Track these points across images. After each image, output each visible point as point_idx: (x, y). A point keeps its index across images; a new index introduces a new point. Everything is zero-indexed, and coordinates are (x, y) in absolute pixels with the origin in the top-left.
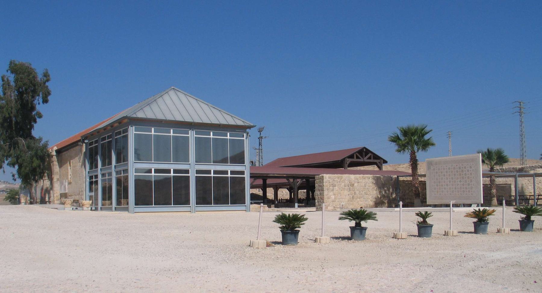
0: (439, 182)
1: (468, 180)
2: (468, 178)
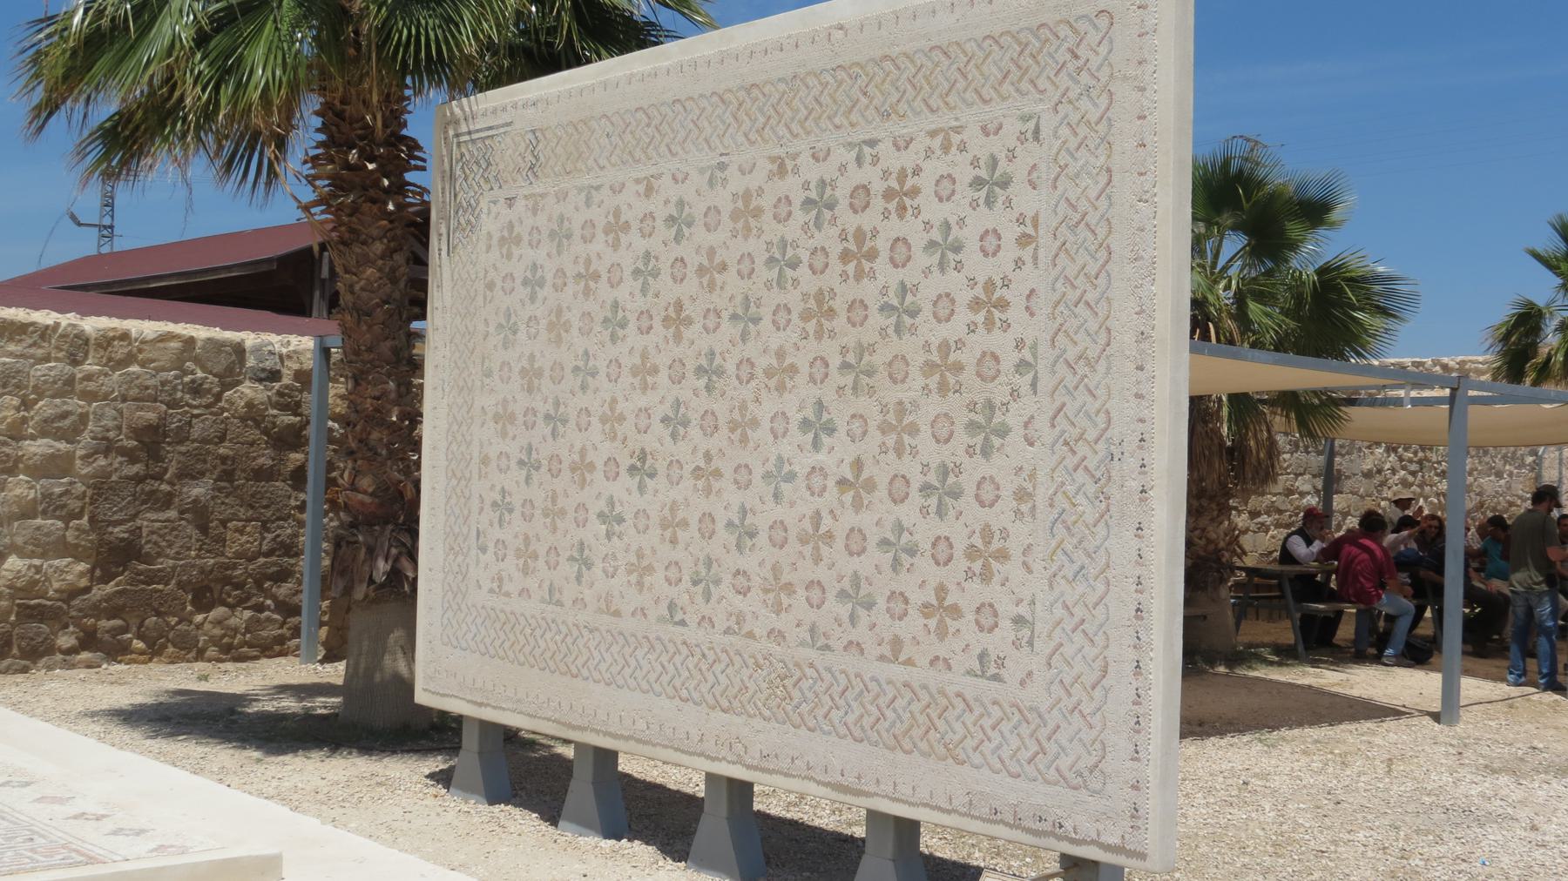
1: (932, 406)
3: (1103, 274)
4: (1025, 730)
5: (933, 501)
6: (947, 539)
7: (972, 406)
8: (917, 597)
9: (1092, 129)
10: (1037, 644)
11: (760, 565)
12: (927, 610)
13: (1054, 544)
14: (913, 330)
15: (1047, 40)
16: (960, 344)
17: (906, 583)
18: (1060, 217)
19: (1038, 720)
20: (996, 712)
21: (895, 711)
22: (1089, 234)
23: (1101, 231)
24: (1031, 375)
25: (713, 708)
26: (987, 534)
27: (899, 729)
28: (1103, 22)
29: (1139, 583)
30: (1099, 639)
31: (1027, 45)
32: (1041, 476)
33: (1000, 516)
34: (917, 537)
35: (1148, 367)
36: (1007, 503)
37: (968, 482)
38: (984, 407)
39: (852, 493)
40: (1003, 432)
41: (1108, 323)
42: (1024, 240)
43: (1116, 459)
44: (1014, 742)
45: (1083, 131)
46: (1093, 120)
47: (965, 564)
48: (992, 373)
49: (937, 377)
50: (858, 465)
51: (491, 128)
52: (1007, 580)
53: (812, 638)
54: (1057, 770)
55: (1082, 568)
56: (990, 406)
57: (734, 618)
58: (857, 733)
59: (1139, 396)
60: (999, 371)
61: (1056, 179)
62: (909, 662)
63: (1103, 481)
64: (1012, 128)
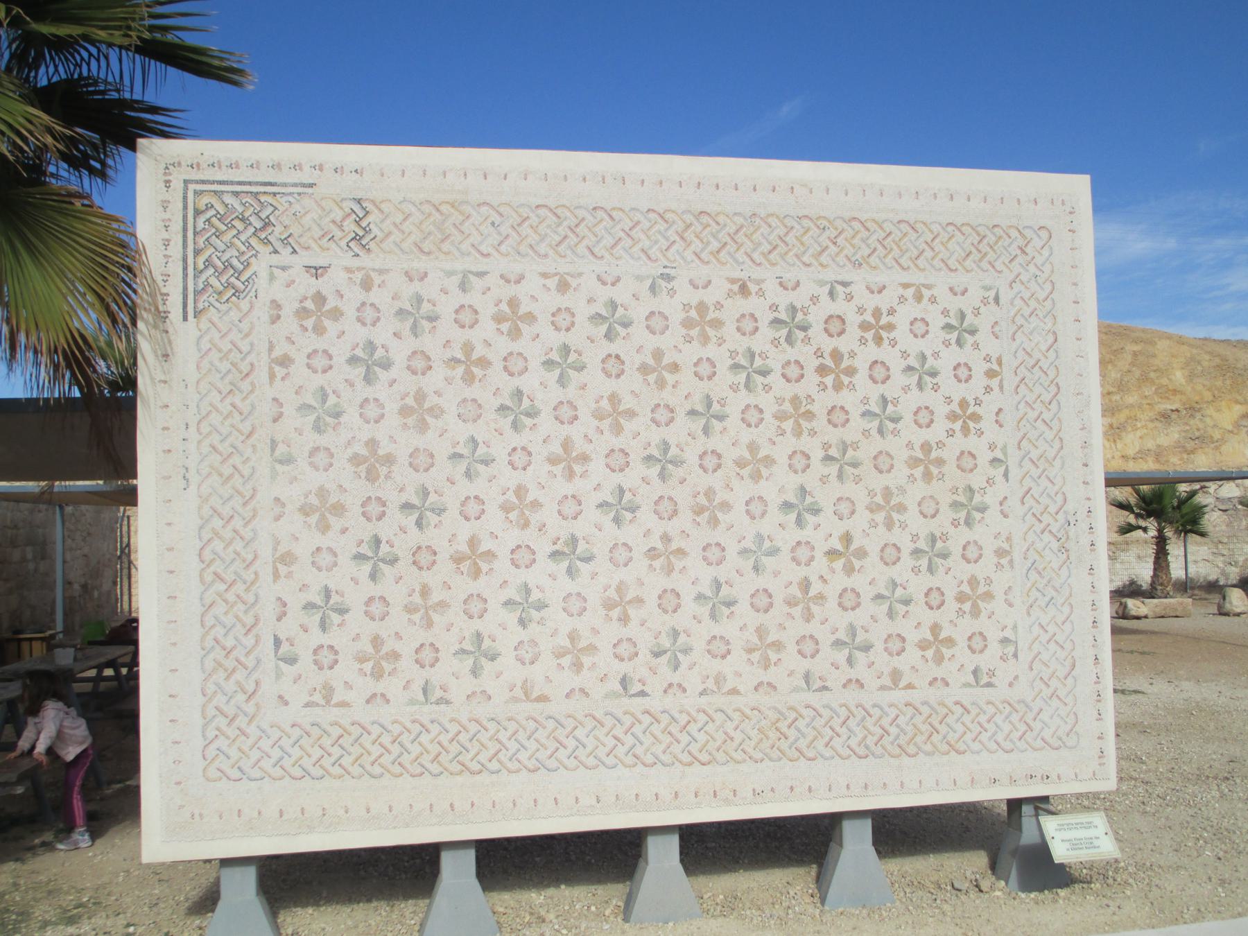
1: (918, 491)
3: (1054, 402)
4: (1015, 718)
5: (924, 562)
6: (938, 589)
7: (955, 490)
8: (913, 637)
9: (1039, 303)
12: (923, 646)
13: (1029, 585)
15: (1000, 237)
16: (940, 445)
17: (904, 627)
20: (991, 710)
21: (898, 726)
22: (1043, 375)
23: (1052, 374)
24: (1004, 468)
25: (690, 764)
26: (973, 582)
28: (1044, 234)
29: (1094, 605)
30: (1068, 645)
31: (984, 237)
33: (984, 569)
35: (1090, 464)
36: (989, 559)
38: (965, 490)
39: (843, 560)
40: (982, 509)
41: (1061, 434)
42: (991, 374)
43: (1072, 525)
44: (1007, 727)
45: (1033, 304)
46: (1041, 299)
47: (956, 606)
48: (970, 466)
49: (921, 469)
50: (847, 538)
52: (993, 613)
53: (808, 685)
54: (1043, 739)
56: (970, 490)
57: (711, 680)
58: (862, 751)
59: (1085, 483)
60: (976, 464)
61: (1014, 334)
62: (910, 686)
63: (1063, 540)
64: (975, 295)
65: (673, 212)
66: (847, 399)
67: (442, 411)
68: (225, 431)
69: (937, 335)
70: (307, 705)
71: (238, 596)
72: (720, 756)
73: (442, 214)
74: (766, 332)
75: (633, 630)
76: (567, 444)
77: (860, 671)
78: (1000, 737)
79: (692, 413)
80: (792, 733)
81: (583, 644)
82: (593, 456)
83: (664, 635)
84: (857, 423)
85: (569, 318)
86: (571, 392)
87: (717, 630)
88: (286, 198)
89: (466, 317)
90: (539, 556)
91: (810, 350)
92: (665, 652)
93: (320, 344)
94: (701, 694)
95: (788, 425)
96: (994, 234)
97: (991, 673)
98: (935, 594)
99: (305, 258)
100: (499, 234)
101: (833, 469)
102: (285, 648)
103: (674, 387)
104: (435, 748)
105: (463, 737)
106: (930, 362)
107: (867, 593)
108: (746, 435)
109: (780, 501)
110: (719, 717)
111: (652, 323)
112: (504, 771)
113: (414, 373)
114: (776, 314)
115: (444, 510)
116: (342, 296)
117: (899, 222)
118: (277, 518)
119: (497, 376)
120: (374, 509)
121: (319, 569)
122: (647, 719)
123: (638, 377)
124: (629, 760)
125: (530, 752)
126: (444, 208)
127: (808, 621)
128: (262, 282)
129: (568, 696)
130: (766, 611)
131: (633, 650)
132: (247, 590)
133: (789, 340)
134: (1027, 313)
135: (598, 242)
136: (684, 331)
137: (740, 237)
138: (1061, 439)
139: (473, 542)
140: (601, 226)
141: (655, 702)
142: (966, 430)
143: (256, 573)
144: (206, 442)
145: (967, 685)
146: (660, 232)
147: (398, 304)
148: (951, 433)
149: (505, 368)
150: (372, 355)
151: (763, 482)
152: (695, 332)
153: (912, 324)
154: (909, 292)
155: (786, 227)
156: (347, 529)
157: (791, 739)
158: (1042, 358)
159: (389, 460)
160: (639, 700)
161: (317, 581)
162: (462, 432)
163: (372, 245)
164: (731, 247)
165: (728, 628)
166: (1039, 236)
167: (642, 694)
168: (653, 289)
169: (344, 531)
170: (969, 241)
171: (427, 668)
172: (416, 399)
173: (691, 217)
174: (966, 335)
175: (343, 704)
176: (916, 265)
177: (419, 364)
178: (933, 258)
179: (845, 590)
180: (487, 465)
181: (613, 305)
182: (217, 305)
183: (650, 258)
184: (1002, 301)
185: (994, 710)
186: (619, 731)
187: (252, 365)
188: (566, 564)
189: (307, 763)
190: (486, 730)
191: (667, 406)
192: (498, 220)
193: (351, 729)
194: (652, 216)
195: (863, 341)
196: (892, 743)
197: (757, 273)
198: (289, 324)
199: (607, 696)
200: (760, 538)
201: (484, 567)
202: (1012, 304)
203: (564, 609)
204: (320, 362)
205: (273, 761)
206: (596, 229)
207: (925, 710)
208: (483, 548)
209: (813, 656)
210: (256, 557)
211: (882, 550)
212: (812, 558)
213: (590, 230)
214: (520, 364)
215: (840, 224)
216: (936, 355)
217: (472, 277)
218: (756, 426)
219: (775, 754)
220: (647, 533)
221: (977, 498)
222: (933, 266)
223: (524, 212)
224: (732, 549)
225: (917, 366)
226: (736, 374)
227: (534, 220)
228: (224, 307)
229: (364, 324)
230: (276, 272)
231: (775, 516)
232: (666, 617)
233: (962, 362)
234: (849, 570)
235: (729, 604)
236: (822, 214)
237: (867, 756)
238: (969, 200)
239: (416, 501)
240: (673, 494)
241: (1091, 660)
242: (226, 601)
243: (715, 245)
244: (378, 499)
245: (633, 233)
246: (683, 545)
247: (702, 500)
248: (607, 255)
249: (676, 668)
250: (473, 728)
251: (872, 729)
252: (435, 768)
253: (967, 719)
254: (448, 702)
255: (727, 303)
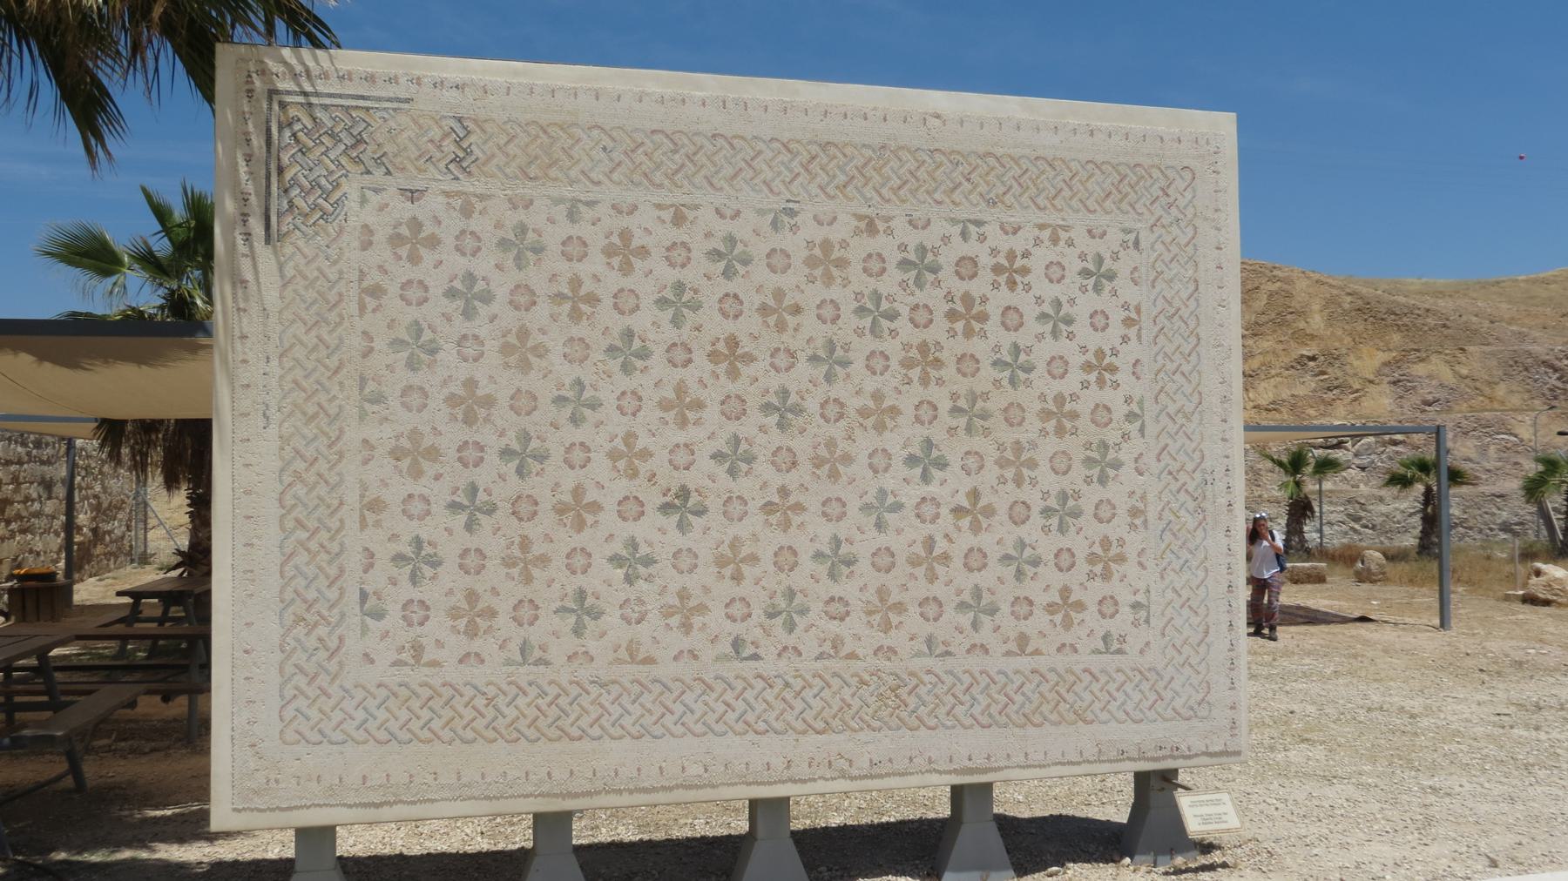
0: (523, 457)
1: (1050, 445)
2: (1059, 415)
3: (1194, 354)
4: (1145, 686)
5: (1055, 521)
7: (1088, 446)
8: (1041, 599)
9: (1181, 249)
10: (1152, 620)
11: (861, 590)
12: (1051, 608)
14: (1028, 384)
16: (1074, 397)
17: (1032, 589)
18: (1159, 308)
19: (1155, 677)
20: (1120, 678)
21: (1023, 694)
23: (1192, 324)
25: (804, 732)
27: (1028, 709)
28: (1187, 175)
30: (1202, 611)
32: (1150, 497)
34: (1039, 551)
36: (1123, 517)
37: (1087, 505)
39: (969, 518)
40: (1117, 465)
42: (1129, 322)
47: (1087, 568)
48: (1105, 420)
49: (1053, 422)
50: (975, 495)
51: (363, 98)
53: (930, 648)
55: (1187, 561)
56: (1104, 446)
57: (828, 644)
58: (985, 720)
59: (1224, 440)
61: (1154, 281)
62: (1037, 652)
64: (1114, 237)
65: (798, 142)
66: (978, 347)
67: (547, 351)
68: (310, 365)
69: (1073, 280)
70: (394, 664)
71: (322, 546)
72: (836, 723)
73: (550, 137)
74: (894, 275)
75: (746, 589)
76: (681, 389)
77: (986, 635)
78: (1129, 707)
79: (814, 359)
80: (912, 701)
81: (692, 603)
82: (708, 402)
83: (779, 594)
84: (987, 372)
85: (684, 254)
86: (686, 333)
87: (836, 590)
88: (379, 114)
89: (574, 249)
90: (648, 509)
91: (940, 293)
92: (780, 613)
93: (415, 273)
94: (817, 659)
95: (915, 373)
96: (1135, 174)
97: (1122, 639)
98: (1065, 556)
99: (401, 180)
100: (611, 160)
101: (962, 421)
102: (371, 602)
103: (796, 330)
104: (532, 712)
105: (563, 701)
106: (1066, 309)
107: (994, 553)
108: (871, 385)
109: (905, 453)
110: (835, 682)
111: (774, 261)
112: (606, 737)
113: (517, 308)
114: (905, 255)
115: (546, 458)
116: (440, 223)
117: (1037, 158)
118: (366, 462)
119: (606, 313)
120: (470, 454)
121: (411, 517)
122: (760, 684)
123: (757, 319)
124: (740, 727)
125: (634, 717)
126: (552, 130)
127: (931, 582)
128: (352, 204)
129: (676, 658)
130: (888, 571)
131: (745, 610)
132: (332, 539)
133: (919, 283)
134: (1167, 260)
135: (716, 173)
136: (807, 271)
137: (869, 171)
138: (1200, 393)
139: (578, 492)
140: (721, 154)
141: (768, 667)
142: (1101, 382)
143: (341, 521)
144: (289, 378)
145: (1097, 651)
146: (783, 163)
147: (500, 233)
148: (1085, 385)
149: (616, 306)
150: (472, 287)
151: (887, 434)
152: (818, 272)
153: (1047, 267)
154: (1046, 234)
155: (917, 161)
156: (441, 475)
157: (911, 707)
158: (1183, 307)
159: (489, 402)
160: (752, 664)
161: (408, 529)
162: (568, 373)
163: (473, 168)
164: (859, 181)
165: (847, 588)
166: (1181, 177)
167: (755, 657)
168: (775, 225)
169: (437, 477)
170: (1109, 180)
171: (526, 626)
172: (518, 338)
173: (818, 149)
174: (1104, 281)
175: (434, 664)
176: (1053, 205)
177: (523, 300)
178: (1071, 198)
179: (971, 550)
180: (594, 409)
181: (731, 240)
182: (303, 228)
183: (771, 191)
184: (1143, 244)
185: (1124, 678)
186: (729, 696)
187: (340, 295)
188: (676, 517)
189: (394, 726)
190: (588, 693)
191: (787, 350)
192: (610, 144)
193: (443, 690)
194: (776, 145)
195: (995, 286)
196: (1017, 712)
197: (886, 210)
198: (381, 253)
199: (717, 659)
200: (882, 493)
201: (589, 519)
202: (1152, 248)
203: (674, 567)
204: (414, 293)
205: (356, 723)
206: (716, 158)
207: (1053, 677)
208: (588, 498)
209: (936, 620)
210: (341, 503)
211: (1011, 508)
212: (937, 516)
213: (709, 159)
214: (632, 301)
215: (972, 159)
216: (1072, 301)
217: (582, 208)
218: (882, 374)
219: (894, 722)
220: (765, 485)
221: (1111, 455)
222: (1070, 207)
223: (639, 137)
224: (853, 506)
225: (1051, 312)
226: (861, 318)
227: (649, 146)
228: (310, 231)
229: (464, 254)
230: (369, 193)
231: (899, 469)
232: (783, 576)
233: (1099, 309)
234: (976, 528)
235: (849, 563)
236: (956, 148)
237: (990, 726)
238: (1110, 137)
239: (516, 446)
240: (791, 444)
241: (1225, 627)
242: (308, 550)
243: (842, 178)
244: (476, 443)
245: (754, 163)
246: (802, 499)
247: (823, 452)
248: (726, 186)
249: (791, 631)
250: (575, 690)
251: (996, 696)
252: (532, 733)
253: (1095, 687)
254: (547, 663)
255: (854, 242)
